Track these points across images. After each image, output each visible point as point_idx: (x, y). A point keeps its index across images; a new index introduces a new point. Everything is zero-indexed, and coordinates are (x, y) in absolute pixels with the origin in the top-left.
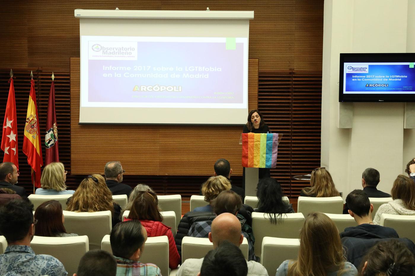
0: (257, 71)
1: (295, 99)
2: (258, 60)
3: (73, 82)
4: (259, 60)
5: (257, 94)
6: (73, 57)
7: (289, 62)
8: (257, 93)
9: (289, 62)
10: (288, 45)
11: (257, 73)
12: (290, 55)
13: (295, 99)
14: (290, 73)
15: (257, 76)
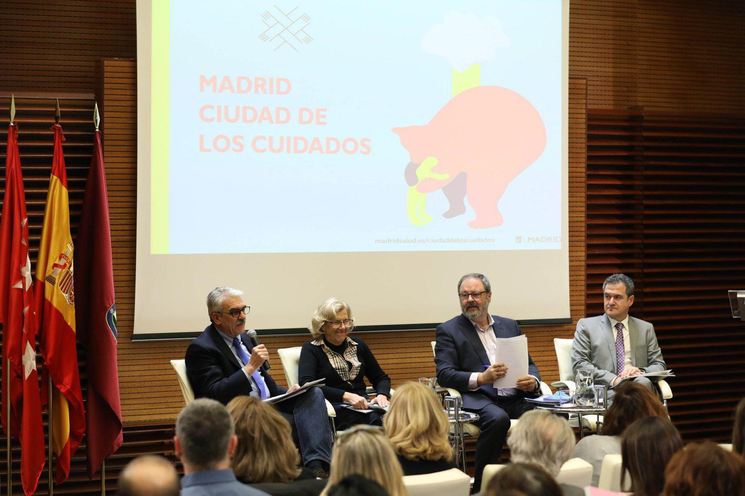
0: (584, 111)
1: (648, 188)
2: (584, 81)
3: (113, 137)
4: (587, 82)
5: (584, 175)
6: (111, 57)
7: (625, 89)
8: (584, 170)
9: (625, 89)
10: (624, 42)
11: (584, 116)
12: (630, 71)
13: (648, 188)
14: (632, 118)
15: (584, 126)
